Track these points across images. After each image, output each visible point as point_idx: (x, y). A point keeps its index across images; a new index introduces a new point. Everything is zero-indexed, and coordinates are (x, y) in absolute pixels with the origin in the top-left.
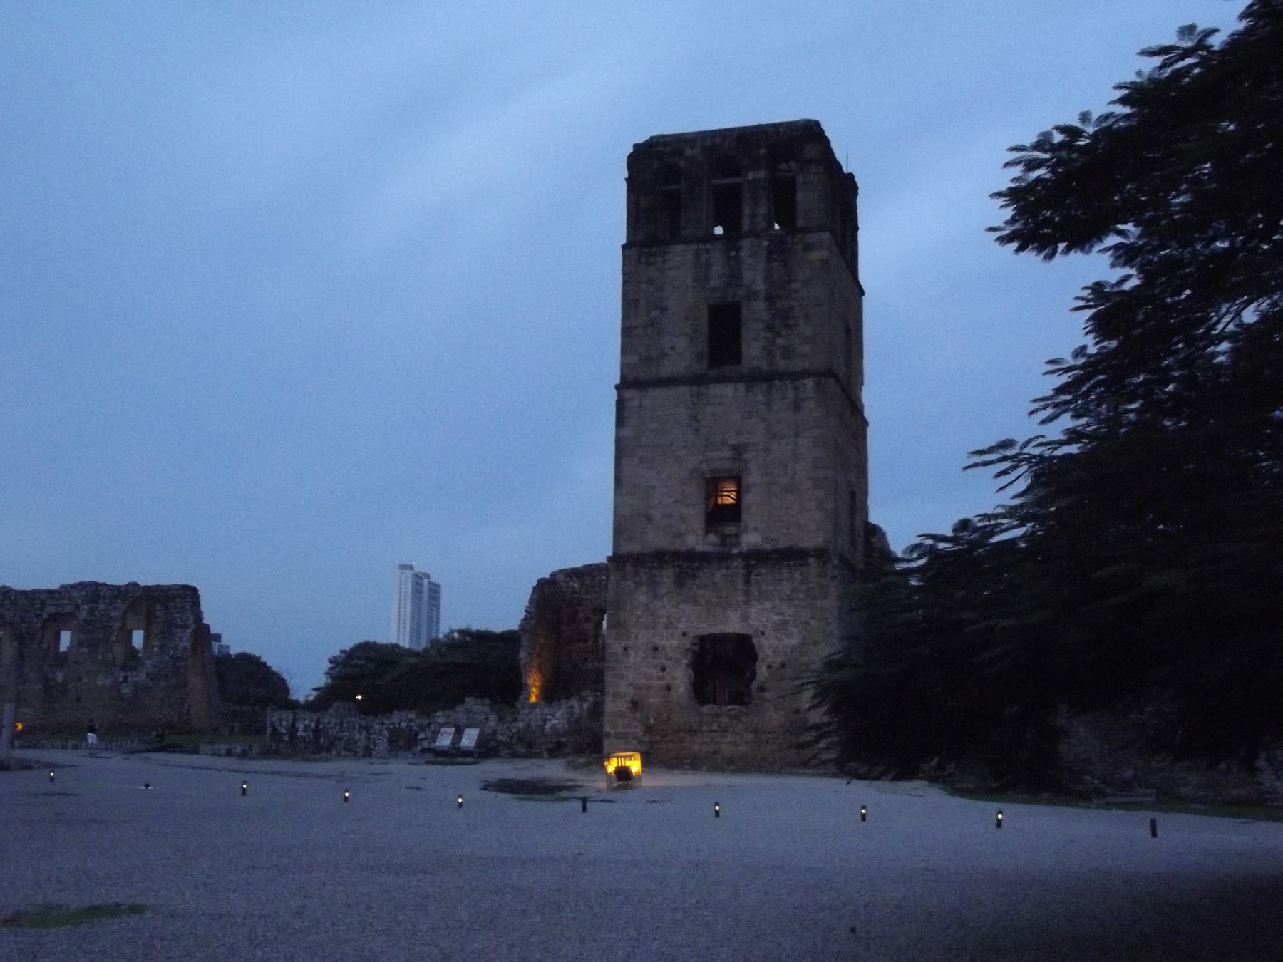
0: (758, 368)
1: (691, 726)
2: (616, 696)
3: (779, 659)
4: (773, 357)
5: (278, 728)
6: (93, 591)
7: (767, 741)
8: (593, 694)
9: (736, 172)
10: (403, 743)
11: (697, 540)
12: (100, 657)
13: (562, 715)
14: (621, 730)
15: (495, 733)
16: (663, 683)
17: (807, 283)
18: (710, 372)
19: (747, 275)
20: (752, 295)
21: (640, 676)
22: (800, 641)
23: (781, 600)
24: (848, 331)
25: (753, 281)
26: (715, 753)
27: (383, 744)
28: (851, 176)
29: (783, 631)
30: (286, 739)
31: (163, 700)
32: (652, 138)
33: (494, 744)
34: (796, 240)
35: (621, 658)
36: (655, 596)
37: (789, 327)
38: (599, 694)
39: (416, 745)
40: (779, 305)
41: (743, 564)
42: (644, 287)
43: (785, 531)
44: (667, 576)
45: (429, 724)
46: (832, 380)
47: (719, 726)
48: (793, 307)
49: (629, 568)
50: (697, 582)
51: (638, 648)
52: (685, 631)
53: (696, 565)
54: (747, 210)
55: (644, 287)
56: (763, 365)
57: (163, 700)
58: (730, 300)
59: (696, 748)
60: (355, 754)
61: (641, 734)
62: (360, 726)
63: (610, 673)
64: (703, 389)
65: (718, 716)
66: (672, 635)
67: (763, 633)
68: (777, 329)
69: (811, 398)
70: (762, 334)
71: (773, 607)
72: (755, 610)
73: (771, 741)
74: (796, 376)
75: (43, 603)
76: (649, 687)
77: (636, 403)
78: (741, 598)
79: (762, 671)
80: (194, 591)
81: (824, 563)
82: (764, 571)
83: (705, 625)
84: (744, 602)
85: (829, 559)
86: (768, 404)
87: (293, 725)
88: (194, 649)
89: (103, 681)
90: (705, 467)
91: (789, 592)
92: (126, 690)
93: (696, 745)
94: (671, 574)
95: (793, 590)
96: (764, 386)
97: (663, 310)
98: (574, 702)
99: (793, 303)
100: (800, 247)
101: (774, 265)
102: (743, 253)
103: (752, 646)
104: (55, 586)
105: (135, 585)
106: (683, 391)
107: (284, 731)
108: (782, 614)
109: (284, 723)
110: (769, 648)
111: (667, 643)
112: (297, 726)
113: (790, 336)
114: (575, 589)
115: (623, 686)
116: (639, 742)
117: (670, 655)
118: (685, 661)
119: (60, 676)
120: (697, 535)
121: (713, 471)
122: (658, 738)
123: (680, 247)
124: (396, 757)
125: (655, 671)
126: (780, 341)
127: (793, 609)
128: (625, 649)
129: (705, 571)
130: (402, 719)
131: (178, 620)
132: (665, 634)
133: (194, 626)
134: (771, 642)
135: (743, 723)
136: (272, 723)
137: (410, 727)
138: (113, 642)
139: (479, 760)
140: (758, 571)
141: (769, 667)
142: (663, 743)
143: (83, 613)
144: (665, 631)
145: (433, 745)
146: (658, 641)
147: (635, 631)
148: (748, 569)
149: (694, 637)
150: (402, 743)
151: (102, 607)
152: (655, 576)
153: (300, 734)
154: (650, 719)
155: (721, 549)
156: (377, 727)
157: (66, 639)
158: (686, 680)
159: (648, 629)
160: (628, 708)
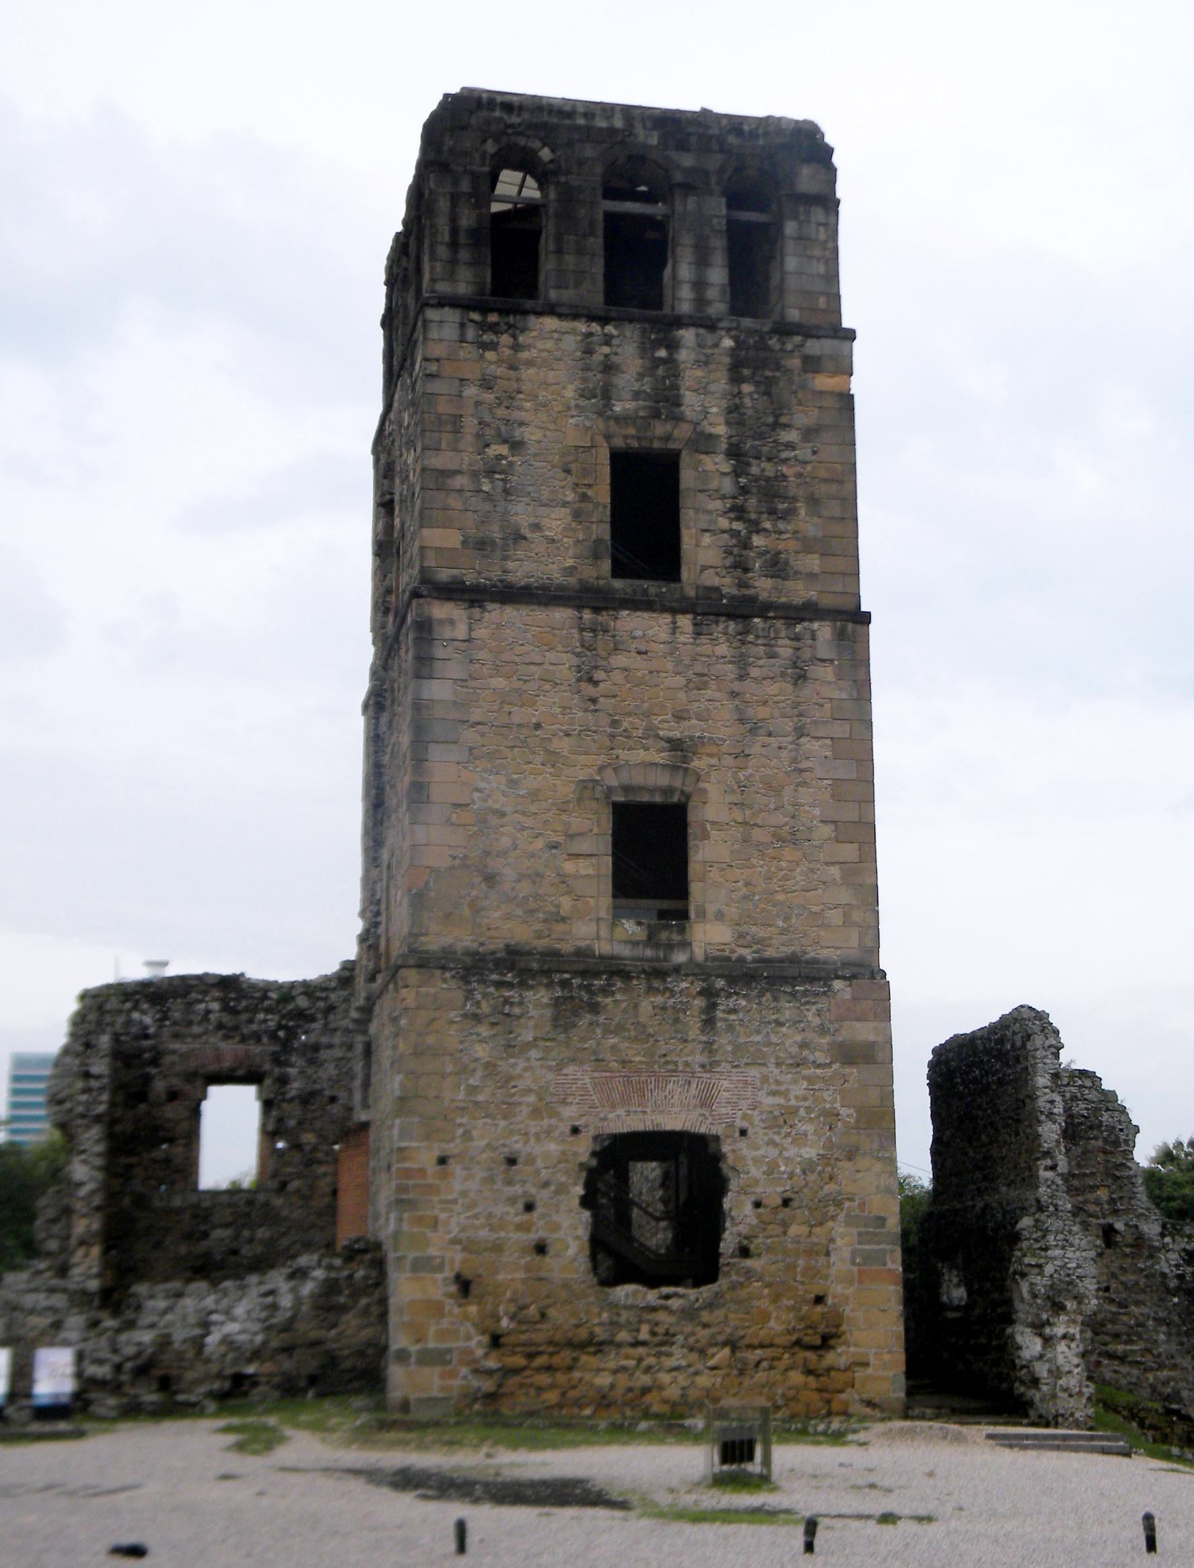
0: (717, 590)
3: (780, 1189)
4: (746, 570)
7: (758, 1364)
8: (325, 1262)
14: (432, 1345)
16: (534, 1236)
17: (809, 433)
18: (618, 584)
20: (703, 442)
21: (477, 1222)
22: (822, 1152)
23: (778, 1065)
25: (706, 413)
26: (645, 1390)
29: (786, 1129)
34: (789, 347)
35: (430, 1181)
37: (772, 512)
40: (755, 470)
42: (471, 391)
43: (781, 924)
44: (538, 1000)
47: (653, 1334)
48: (784, 477)
50: (601, 1019)
51: (472, 1159)
52: (577, 1123)
54: (685, 271)
55: (471, 391)
58: (656, 445)
59: (604, 1380)
61: (480, 1352)
63: (406, 1215)
64: (603, 618)
65: (654, 1309)
66: (548, 1132)
67: (743, 1133)
68: (753, 516)
70: (724, 523)
71: (765, 1079)
72: (726, 1084)
73: (765, 1364)
76: (497, 1248)
78: (699, 1058)
82: (744, 1003)
83: (621, 1111)
84: (703, 1066)
86: (742, 663)
90: (611, 780)
91: (794, 1050)
94: (545, 1000)
95: (804, 1045)
96: (732, 626)
97: (517, 446)
99: (785, 469)
100: (795, 363)
101: (747, 388)
102: (683, 355)
103: (718, 1158)
106: (562, 615)
108: (785, 1094)
111: (537, 1150)
113: (781, 533)
116: (476, 1371)
117: (545, 1174)
118: (579, 1190)
121: (627, 789)
122: (520, 1361)
123: (550, 323)
125: (512, 1211)
126: (757, 541)
127: (805, 1084)
128: (442, 1161)
129: (618, 997)
132: (533, 1130)
134: (761, 1152)
135: (705, 1326)
140: (731, 1003)
141: (757, 1205)
142: (528, 1372)
144: (533, 1123)
146: (517, 1145)
147: (464, 1120)
148: (709, 993)
152: (507, 1001)
154: (498, 1320)
155: (649, 953)
159: (494, 1119)
160: (450, 1295)
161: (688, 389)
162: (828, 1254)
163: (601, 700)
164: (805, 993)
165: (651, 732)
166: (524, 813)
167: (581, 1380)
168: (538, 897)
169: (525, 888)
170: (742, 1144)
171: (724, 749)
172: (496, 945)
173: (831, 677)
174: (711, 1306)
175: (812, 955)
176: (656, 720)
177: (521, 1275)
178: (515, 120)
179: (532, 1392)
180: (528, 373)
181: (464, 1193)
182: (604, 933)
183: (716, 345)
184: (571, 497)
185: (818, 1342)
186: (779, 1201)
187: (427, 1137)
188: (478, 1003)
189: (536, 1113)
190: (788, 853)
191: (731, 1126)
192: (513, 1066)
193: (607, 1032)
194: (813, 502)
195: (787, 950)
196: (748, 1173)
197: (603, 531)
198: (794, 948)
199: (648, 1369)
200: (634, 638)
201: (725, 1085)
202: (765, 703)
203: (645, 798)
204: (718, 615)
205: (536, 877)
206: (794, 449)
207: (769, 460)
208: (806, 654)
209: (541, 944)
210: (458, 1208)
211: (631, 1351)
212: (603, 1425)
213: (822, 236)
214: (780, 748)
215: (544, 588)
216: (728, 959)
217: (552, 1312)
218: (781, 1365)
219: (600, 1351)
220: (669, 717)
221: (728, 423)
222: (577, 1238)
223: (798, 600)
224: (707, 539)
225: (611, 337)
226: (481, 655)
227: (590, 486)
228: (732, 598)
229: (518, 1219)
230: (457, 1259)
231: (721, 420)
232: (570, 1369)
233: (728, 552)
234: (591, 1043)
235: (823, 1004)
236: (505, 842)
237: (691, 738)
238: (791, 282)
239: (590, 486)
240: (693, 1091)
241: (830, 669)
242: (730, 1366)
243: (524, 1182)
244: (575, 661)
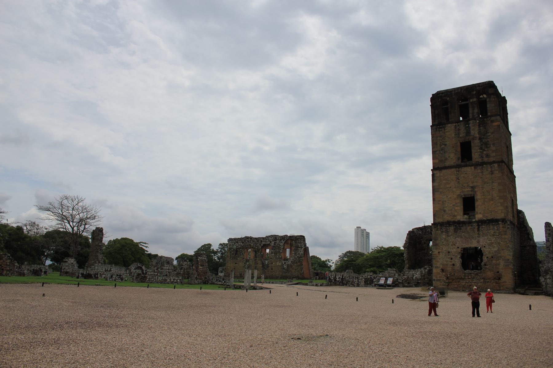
0: (478, 161)
1: (462, 277)
2: (436, 267)
3: (491, 255)
4: (483, 157)
5: (331, 278)
6: (275, 238)
7: (488, 282)
8: (429, 267)
9: (466, 99)
10: (369, 283)
11: (460, 217)
12: (278, 257)
13: (419, 274)
14: (438, 278)
15: (397, 279)
16: (452, 263)
17: (492, 133)
18: (462, 163)
19: (472, 132)
20: (474, 138)
21: (444, 261)
23: (490, 236)
24: (507, 147)
26: (470, 285)
27: (363, 283)
28: (504, 97)
29: (492, 246)
30: (333, 281)
31: (296, 269)
32: (438, 92)
33: (397, 283)
34: (488, 120)
36: (448, 236)
37: (487, 147)
38: (430, 267)
39: (373, 283)
40: (483, 141)
41: (476, 224)
42: (439, 138)
43: (490, 213)
44: (452, 228)
45: (377, 277)
46: (504, 164)
47: (471, 277)
48: (488, 141)
49: (439, 227)
50: (461, 231)
53: (461, 225)
54: (471, 111)
55: (439, 138)
56: (480, 160)
57: (296, 269)
58: (467, 140)
59: (464, 284)
60: (354, 286)
61: (445, 280)
62: (355, 277)
64: (460, 169)
65: (471, 274)
67: (485, 247)
68: (484, 149)
69: (496, 170)
71: (488, 238)
73: (489, 282)
74: (491, 163)
75: (261, 241)
76: (447, 265)
77: (438, 175)
79: (485, 259)
80: (304, 237)
81: (505, 223)
82: (484, 226)
83: (465, 244)
84: (477, 237)
85: (506, 222)
86: (482, 172)
87: (335, 277)
88: (304, 254)
89: (279, 264)
90: (462, 194)
91: (493, 233)
92: (285, 266)
93: (463, 283)
95: (494, 232)
96: (480, 167)
97: (445, 145)
98: (422, 269)
99: (488, 140)
100: (489, 122)
102: (470, 125)
104: (264, 237)
105: (286, 236)
106: (453, 170)
107: (333, 279)
109: (333, 276)
110: (487, 252)
111: (452, 251)
112: (336, 277)
113: (488, 150)
114: (420, 234)
115: (438, 265)
117: (454, 254)
118: (459, 256)
119: (267, 262)
120: (461, 216)
121: (465, 195)
122: (451, 281)
123: (449, 125)
124: (367, 287)
125: (449, 259)
126: (485, 152)
127: (495, 238)
128: (439, 253)
130: (368, 275)
131: (299, 246)
133: (304, 248)
134: (487, 250)
135: (480, 276)
136: (329, 276)
137: (371, 278)
138: (281, 252)
139: (393, 288)
140: (482, 227)
141: (487, 258)
143: (272, 244)
145: (378, 283)
148: (478, 226)
149: (461, 248)
150: (368, 283)
154: (448, 275)
156: (360, 277)
157: (268, 251)
158: (459, 262)
161: (472, 130)
162: (499, 265)
163: (460, 182)
164: (494, 224)
165: (468, 186)
166: (449, 201)
167: (460, 284)
168: (452, 213)
169: (450, 212)
170: (485, 248)
171: (480, 187)
172: (445, 221)
173: (497, 173)
174: (480, 273)
175: (496, 218)
176: (469, 184)
177: (451, 269)
178: (443, 95)
179: (453, 285)
180: (447, 133)
181: (442, 257)
182: (462, 218)
183: (476, 122)
184: (454, 151)
185: (498, 278)
186: (491, 257)
187: (436, 249)
188: (443, 230)
189: (452, 245)
190: (492, 202)
191: (482, 246)
192: (448, 238)
193: (463, 232)
194: (494, 144)
195: (492, 218)
196: (485, 253)
197: (460, 156)
198: (493, 217)
199: (471, 282)
200: (465, 171)
201: (481, 240)
202: (486, 178)
203: (467, 196)
204: (478, 165)
205: (451, 210)
206: (490, 136)
207: (486, 139)
208: (493, 169)
209: (452, 220)
210: (441, 259)
211: (468, 280)
212: (461, 290)
213: (493, 100)
214: (489, 185)
215: (451, 166)
216: (482, 220)
217: (456, 274)
218: (492, 282)
219: (463, 280)
220: (471, 183)
221: (479, 134)
222: (459, 263)
223: (492, 161)
224: (476, 154)
225: (459, 125)
226: (442, 178)
227: (457, 149)
228: (481, 162)
229: (450, 261)
230: (441, 266)
231: (477, 134)
232: (459, 282)
233: (480, 155)
234: (460, 234)
235: (497, 226)
236: (447, 205)
237: (475, 186)
238: (488, 109)
239: (457, 149)
240: (476, 241)
241: (497, 171)
242: (483, 282)
243: (450, 255)
244: (456, 177)
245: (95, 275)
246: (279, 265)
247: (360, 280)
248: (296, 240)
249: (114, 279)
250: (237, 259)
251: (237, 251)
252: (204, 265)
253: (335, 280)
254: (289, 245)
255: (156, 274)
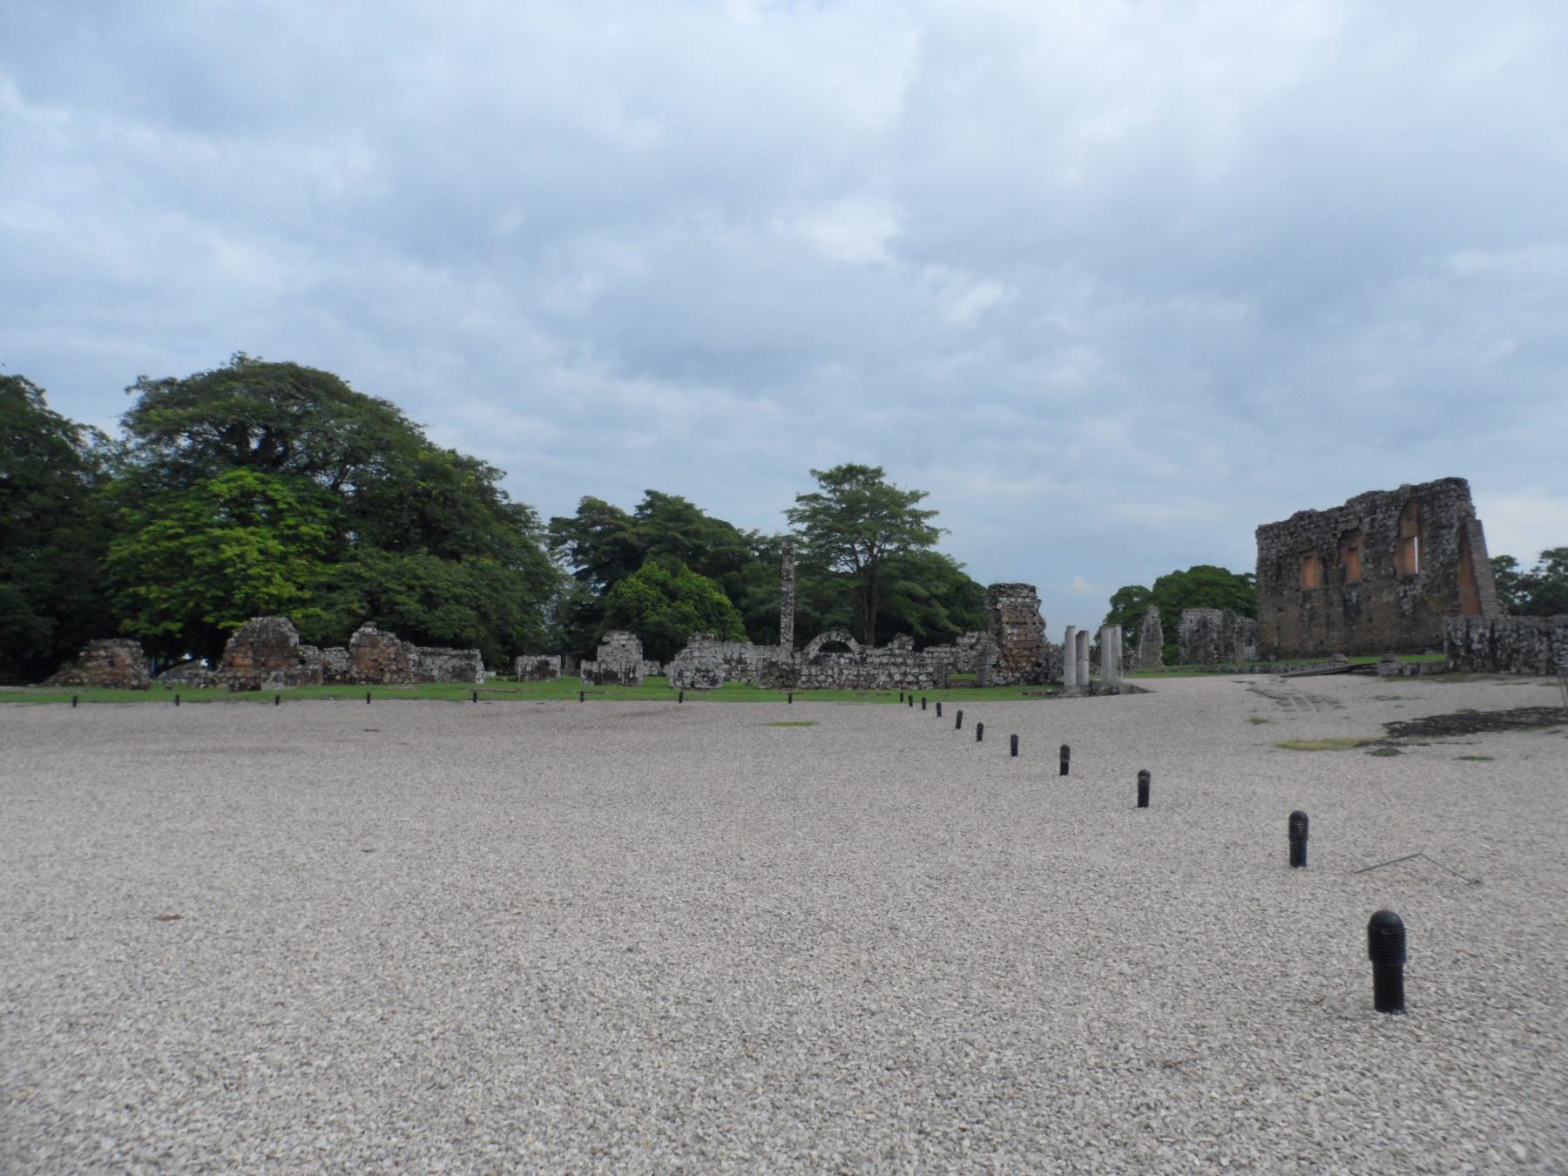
12: (1383, 572)
60: (1537, 674)
62: (1540, 632)
87: (1468, 634)
89: (1388, 597)
104: (1342, 504)
143: (1366, 528)
151: (1380, 516)
153: (1475, 646)
245: (626, 674)
246: (1388, 603)
247: (1556, 645)
248: (1433, 499)
249: (688, 681)
250: (1282, 595)
251: (1279, 568)
252: (1025, 623)
253: (1469, 650)
254: (1413, 522)
255: (900, 660)
